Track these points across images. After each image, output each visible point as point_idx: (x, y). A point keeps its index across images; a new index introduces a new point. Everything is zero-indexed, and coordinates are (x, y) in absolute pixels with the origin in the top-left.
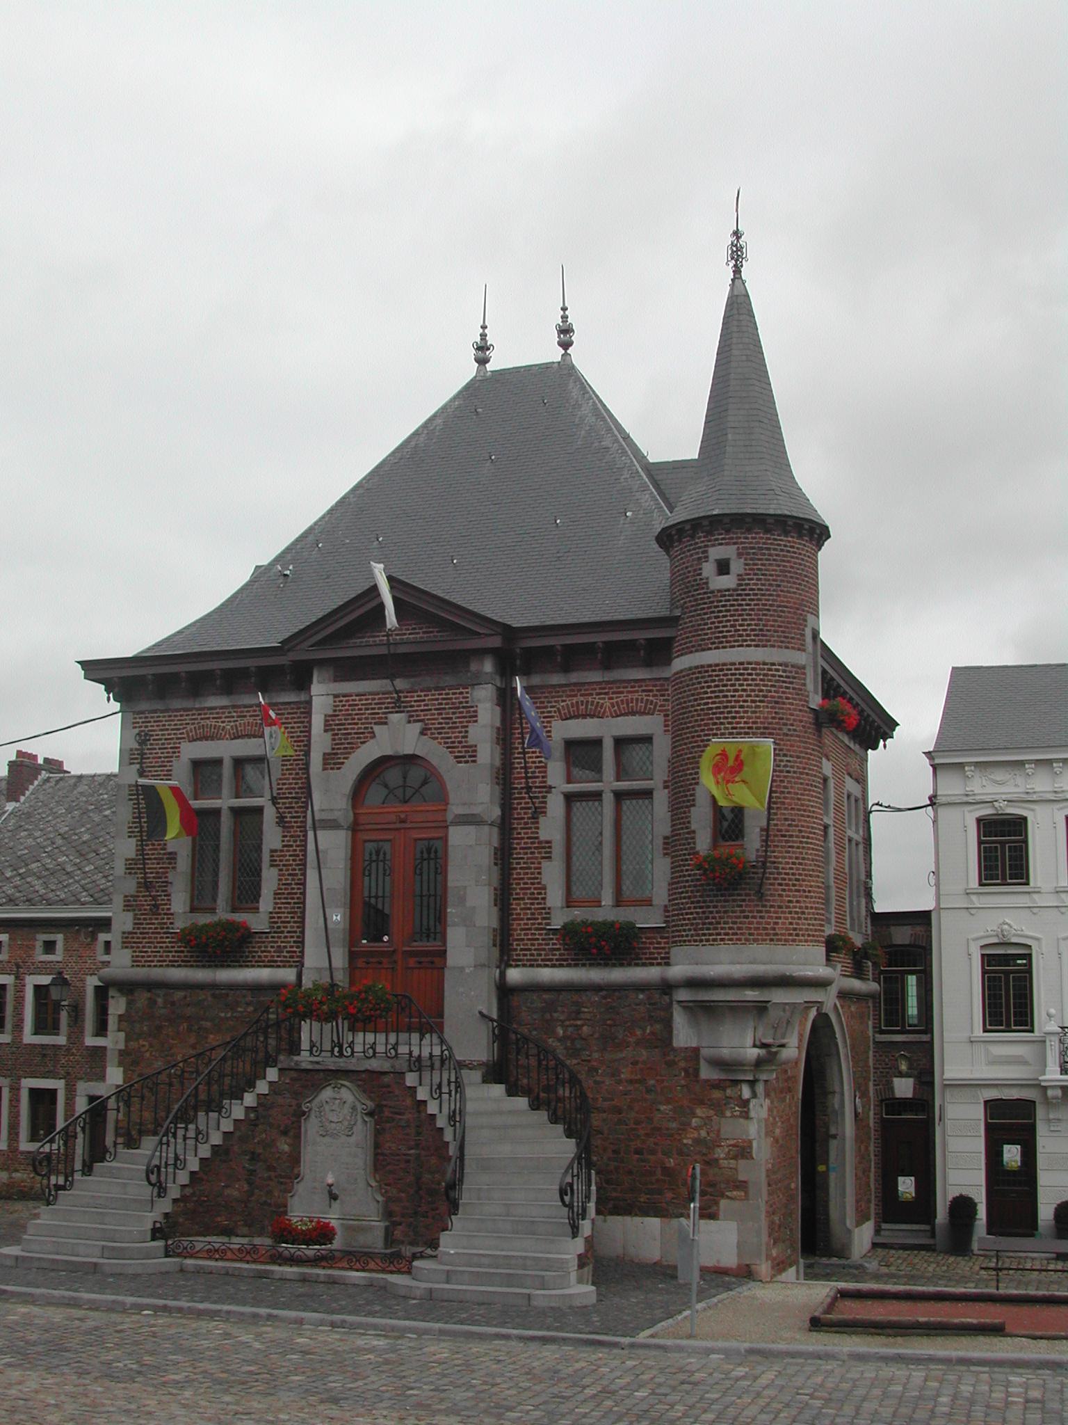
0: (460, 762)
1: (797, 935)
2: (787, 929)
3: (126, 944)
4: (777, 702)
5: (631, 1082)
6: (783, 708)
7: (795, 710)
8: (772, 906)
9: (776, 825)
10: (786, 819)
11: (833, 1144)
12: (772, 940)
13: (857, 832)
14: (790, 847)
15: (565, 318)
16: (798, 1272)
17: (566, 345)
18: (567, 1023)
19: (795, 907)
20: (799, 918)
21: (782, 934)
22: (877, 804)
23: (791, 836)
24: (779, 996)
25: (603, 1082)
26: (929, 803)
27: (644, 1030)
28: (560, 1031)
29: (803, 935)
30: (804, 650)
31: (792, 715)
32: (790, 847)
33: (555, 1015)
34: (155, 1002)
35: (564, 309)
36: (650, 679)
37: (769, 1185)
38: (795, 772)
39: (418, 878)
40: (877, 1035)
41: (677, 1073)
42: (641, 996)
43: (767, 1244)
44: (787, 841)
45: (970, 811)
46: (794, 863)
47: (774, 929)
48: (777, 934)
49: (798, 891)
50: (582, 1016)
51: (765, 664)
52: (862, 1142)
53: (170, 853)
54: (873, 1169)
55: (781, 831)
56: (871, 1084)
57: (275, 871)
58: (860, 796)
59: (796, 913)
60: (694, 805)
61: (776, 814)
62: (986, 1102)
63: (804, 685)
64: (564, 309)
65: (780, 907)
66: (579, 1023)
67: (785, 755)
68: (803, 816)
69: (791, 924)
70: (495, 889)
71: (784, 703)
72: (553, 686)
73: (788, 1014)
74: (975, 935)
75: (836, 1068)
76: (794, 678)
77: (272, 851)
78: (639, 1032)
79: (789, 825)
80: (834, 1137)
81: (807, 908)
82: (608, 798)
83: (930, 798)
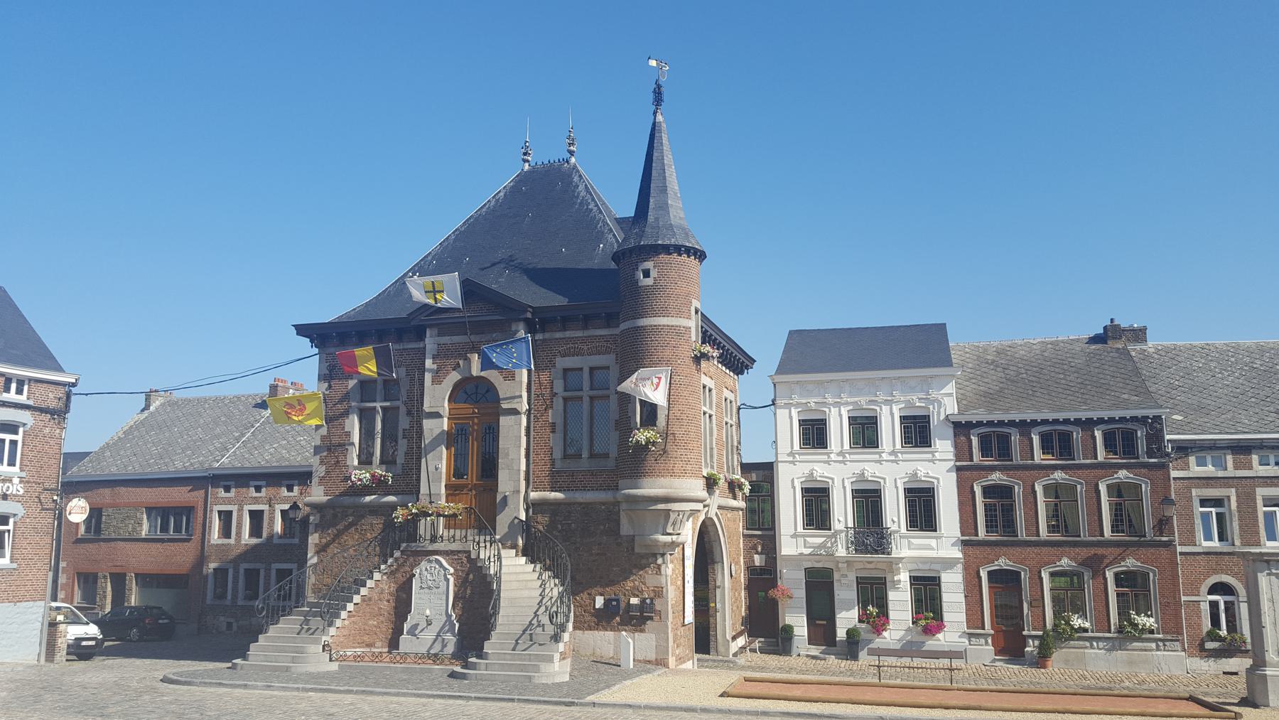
0: (505, 380)
1: (686, 473)
2: (680, 470)
3: (320, 484)
4: (674, 347)
5: (598, 554)
7: (685, 351)
8: (671, 457)
9: (674, 413)
10: (679, 410)
11: (718, 591)
13: (731, 419)
16: (693, 663)
18: (564, 522)
20: (687, 464)
22: (743, 404)
23: (682, 419)
25: (583, 555)
26: (771, 403)
27: (605, 527)
28: (560, 526)
29: (689, 473)
30: (690, 319)
31: (683, 353)
33: (557, 518)
34: (337, 516)
36: (608, 335)
37: (673, 613)
38: (684, 385)
39: (484, 443)
40: (745, 531)
41: (622, 549)
42: (603, 507)
43: (673, 647)
44: (680, 422)
46: (684, 434)
49: (686, 449)
50: (572, 518)
51: (668, 326)
52: (736, 590)
53: (347, 432)
54: (744, 606)
55: (676, 416)
56: (742, 558)
57: (406, 441)
58: (733, 400)
59: (686, 461)
60: (630, 403)
61: (673, 407)
62: (805, 569)
63: (690, 337)
65: (676, 458)
66: (570, 522)
67: (679, 375)
69: (682, 467)
71: (678, 347)
72: (557, 339)
73: (681, 516)
74: (797, 476)
75: (719, 548)
76: (684, 334)
77: (404, 430)
78: (602, 527)
79: (681, 413)
80: (719, 587)
81: (691, 458)
82: (586, 400)
83: (773, 402)
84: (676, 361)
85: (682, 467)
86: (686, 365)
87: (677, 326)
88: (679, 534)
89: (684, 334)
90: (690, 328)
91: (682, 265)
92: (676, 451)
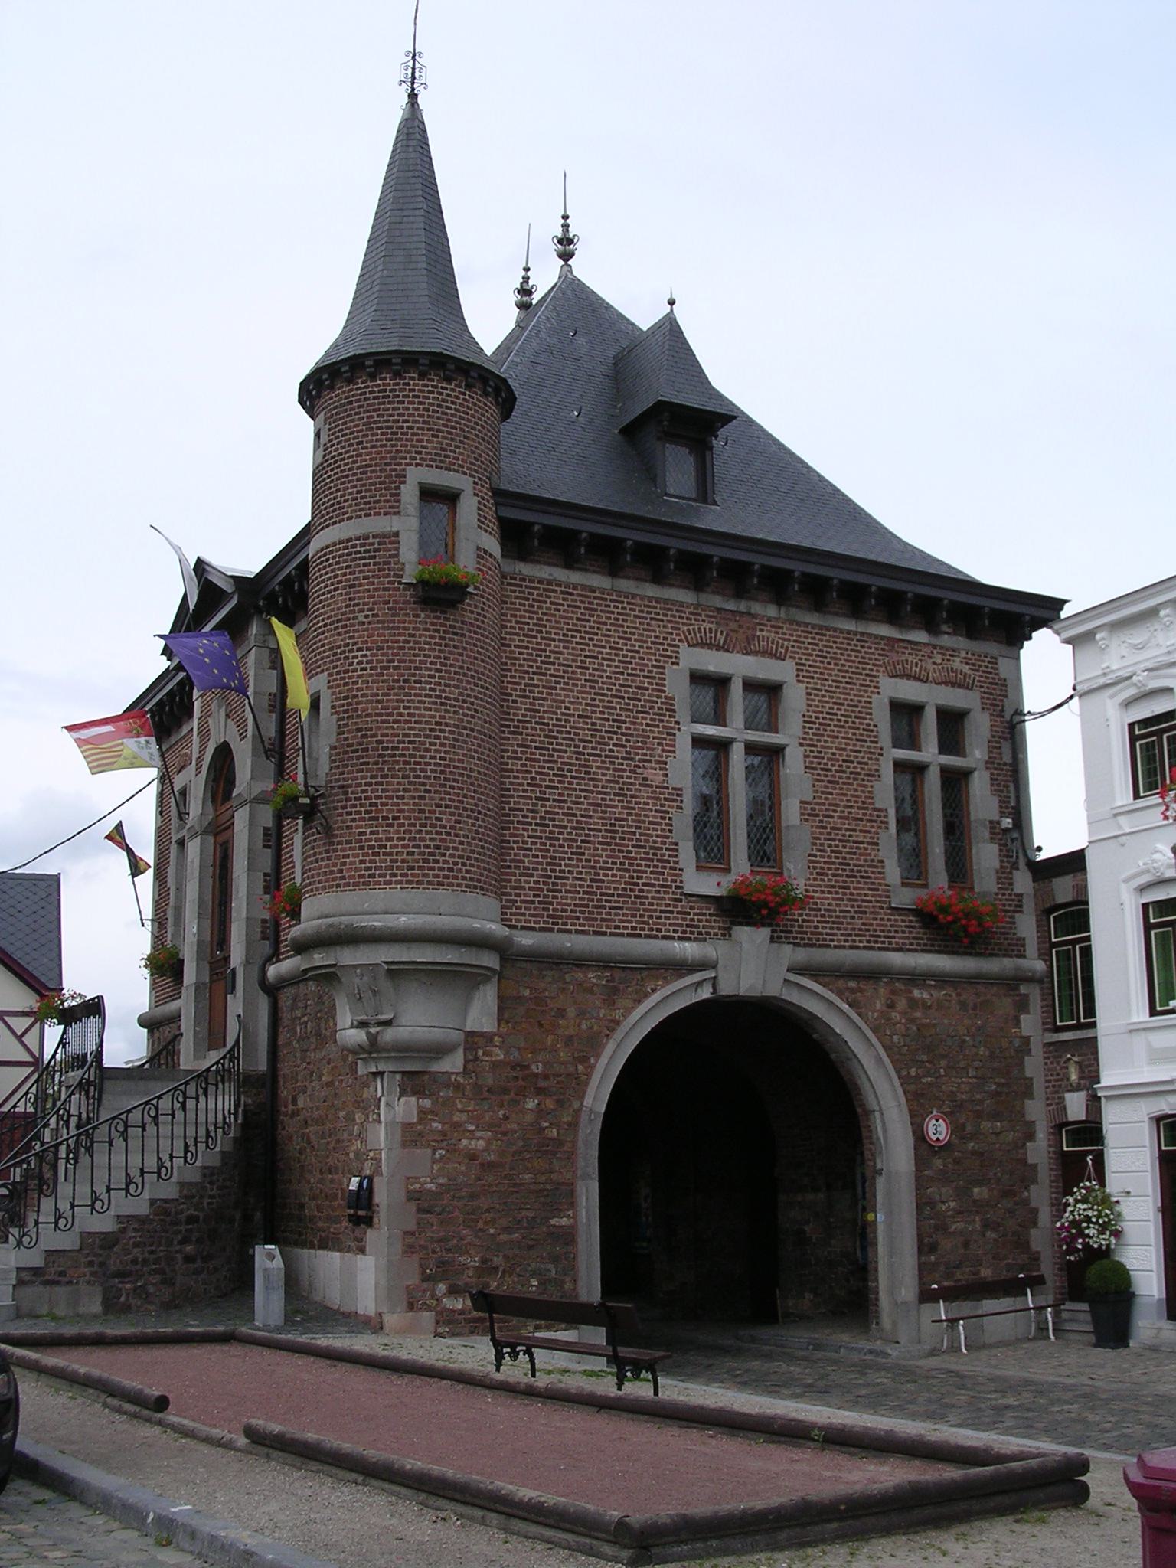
1: (371, 876)
4: (351, 586)
6: (359, 592)
10: (358, 730)
11: (880, 1183)
12: (338, 886)
14: (361, 764)
15: (566, 227)
17: (566, 256)
19: (370, 840)
21: (350, 877)
24: (347, 956)
30: (398, 513)
32: (361, 764)
35: (565, 217)
44: (358, 758)
45: (1111, 697)
47: (341, 871)
48: (344, 878)
49: (376, 818)
51: (341, 542)
59: (372, 847)
64: (565, 217)
65: (348, 842)
68: (388, 722)
69: (362, 862)
70: (265, 875)
71: (361, 585)
74: (1124, 876)
76: (378, 550)
84: (355, 618)
85: (362, 862)
86: (378, 622)
87: (358, 539)
88: (388, 1023)
89: (378, 550)
90: (397, 534)
91: (377, 398)
92: (349, 827)
